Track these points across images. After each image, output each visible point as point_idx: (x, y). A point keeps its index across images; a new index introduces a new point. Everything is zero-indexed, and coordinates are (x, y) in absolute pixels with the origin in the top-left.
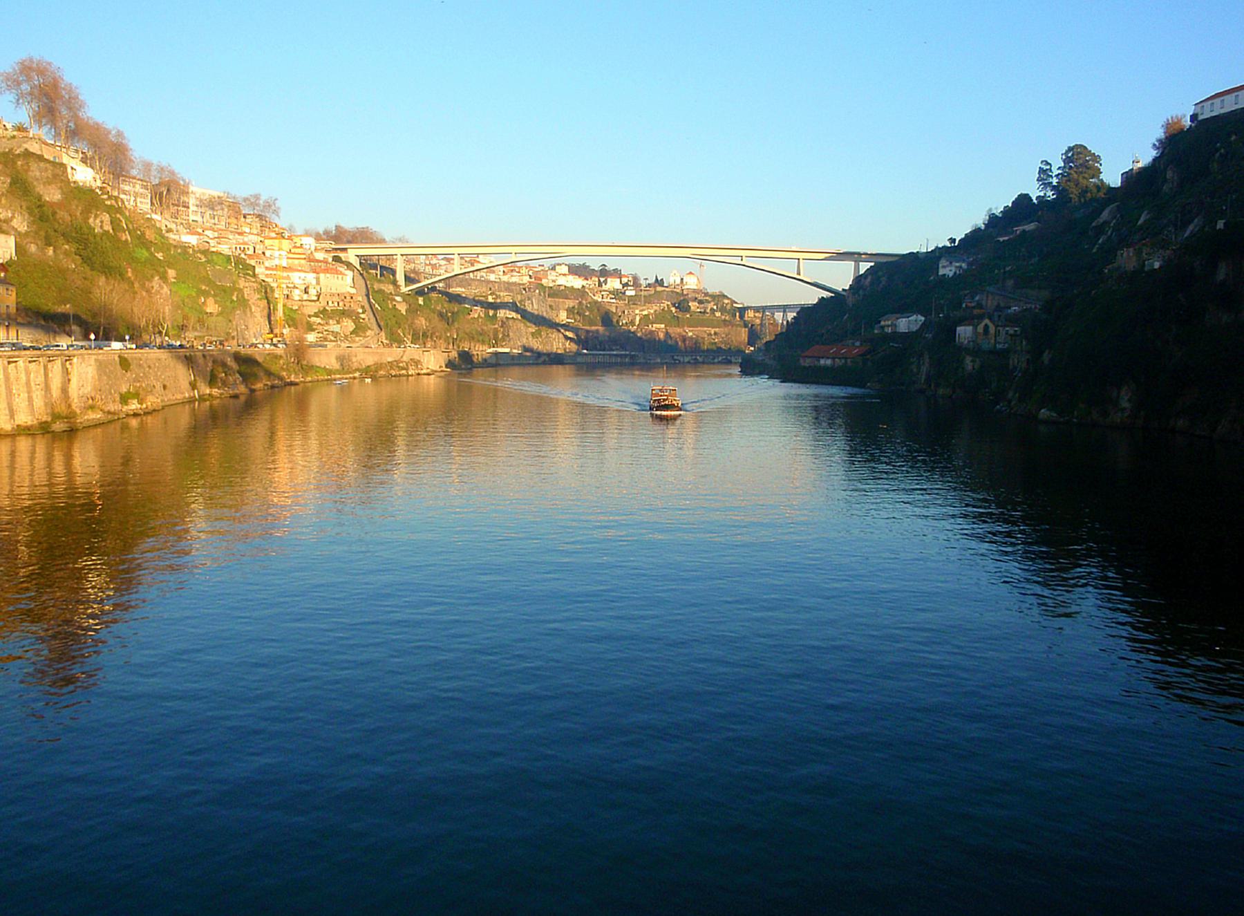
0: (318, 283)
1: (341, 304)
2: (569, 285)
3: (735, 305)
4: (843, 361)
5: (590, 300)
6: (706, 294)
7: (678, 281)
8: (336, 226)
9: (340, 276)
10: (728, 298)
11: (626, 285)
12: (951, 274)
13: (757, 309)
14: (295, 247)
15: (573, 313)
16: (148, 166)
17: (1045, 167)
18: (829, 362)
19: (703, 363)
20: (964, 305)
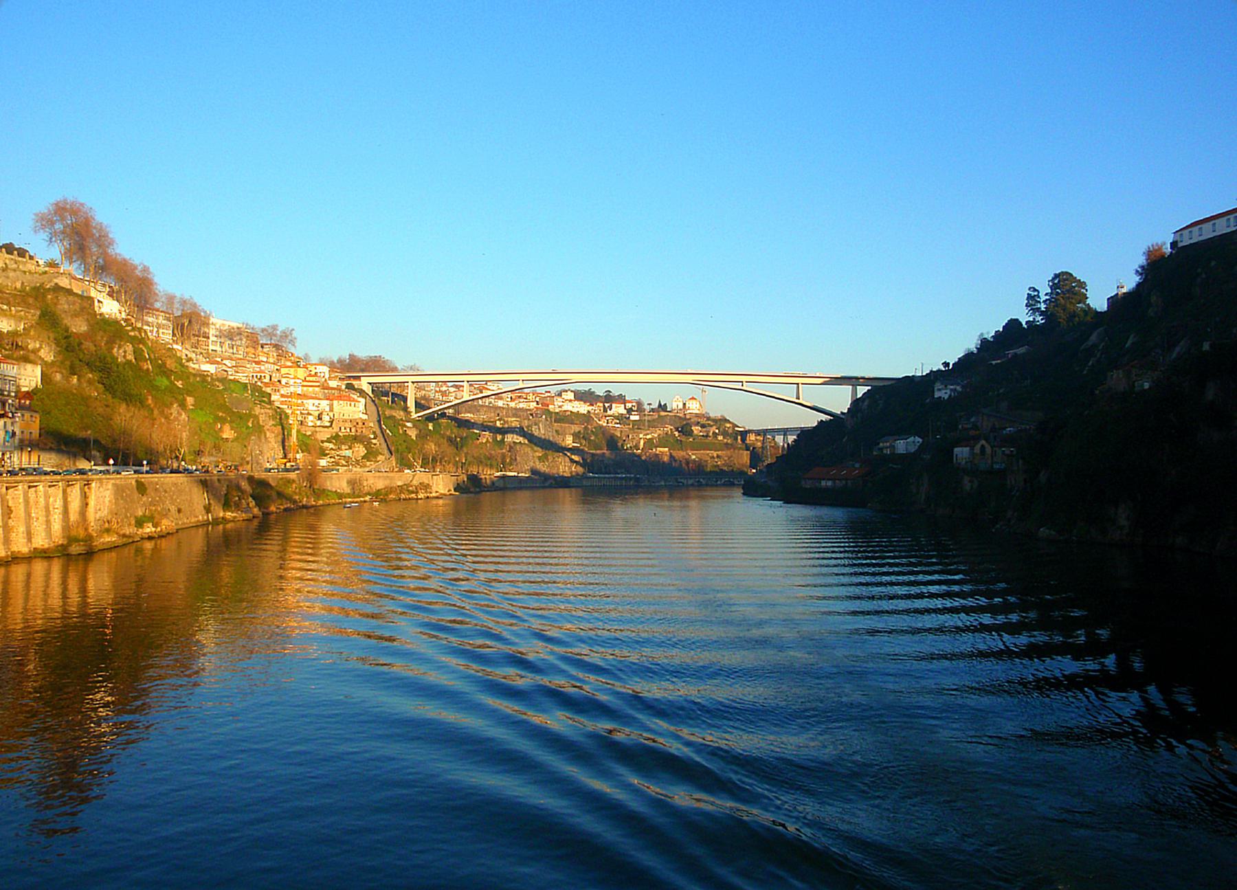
0: (331, 410)
1: (353, 430)
2: (575, 410)
3: (737, 429)
4: (844, 482)
5: (595, 425)
6: (709, 419)
7: (681, 406)
8: (350, 355)
9: (353, 403)
10: (729, 421)
11: (630, 411)
12: (946, 397)
13: (758, 433)
14: (310, 375)
15: (579, 437)
16: (171, 299)
17: (1033, 294)
18: (830, 483)
19: (707, 485)
20: (960, 427)
